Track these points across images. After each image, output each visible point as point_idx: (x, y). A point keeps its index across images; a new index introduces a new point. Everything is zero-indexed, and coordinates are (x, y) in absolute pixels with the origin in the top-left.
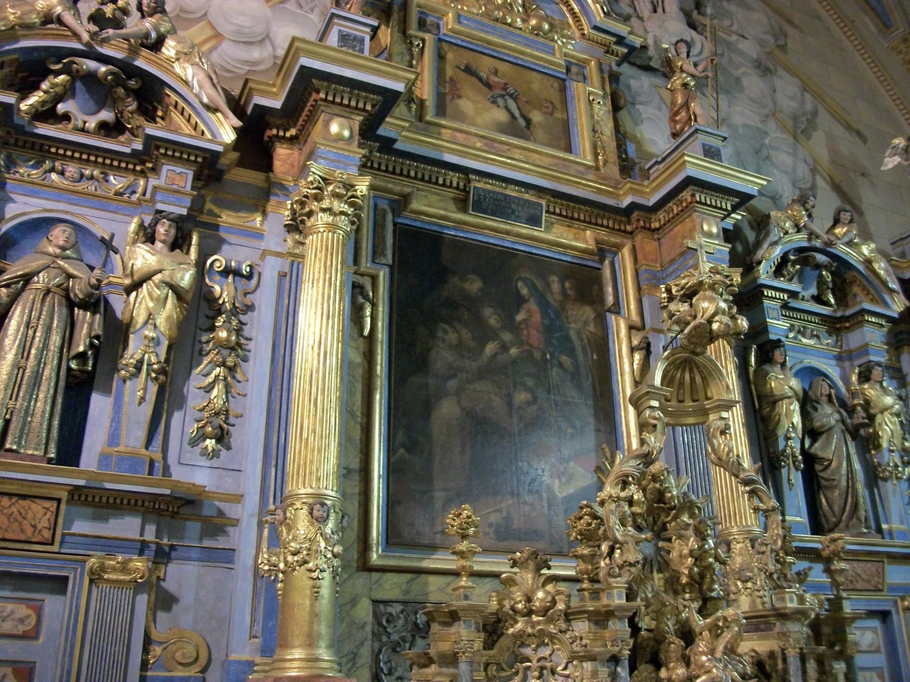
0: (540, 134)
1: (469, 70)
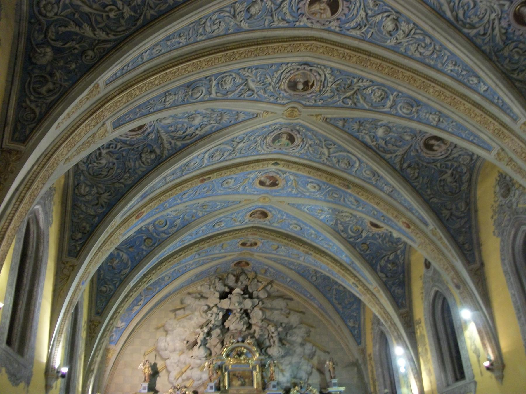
0: (247, 384)
1: (234, 375)
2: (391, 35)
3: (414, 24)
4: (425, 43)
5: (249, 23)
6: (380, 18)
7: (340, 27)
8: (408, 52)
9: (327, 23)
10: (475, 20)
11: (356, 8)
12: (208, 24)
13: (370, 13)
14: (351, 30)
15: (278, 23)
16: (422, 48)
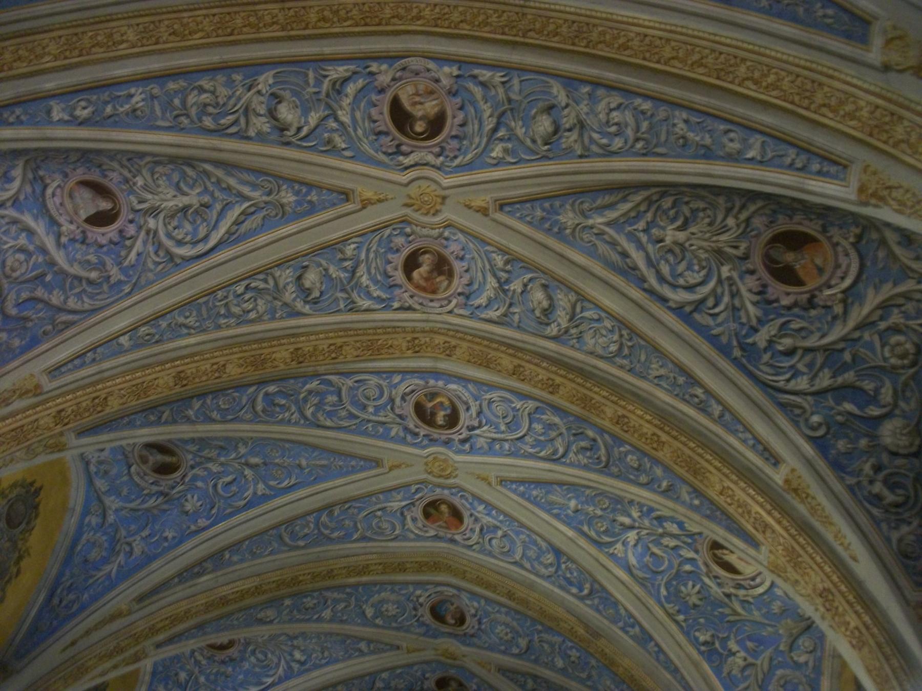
2: (274, 95)
3: (248, 138)
4: (210, 114)
5: (550, 93)
6: (310, 120)
7: (371, 74)
8: (224, 79)
9: (398, 74)
10: (159, 169)
11: (360, 123)
12: (630, 132)
13: (333, 125)
14: (349, 74)
15: (493, 75)
16: (208, 100)
